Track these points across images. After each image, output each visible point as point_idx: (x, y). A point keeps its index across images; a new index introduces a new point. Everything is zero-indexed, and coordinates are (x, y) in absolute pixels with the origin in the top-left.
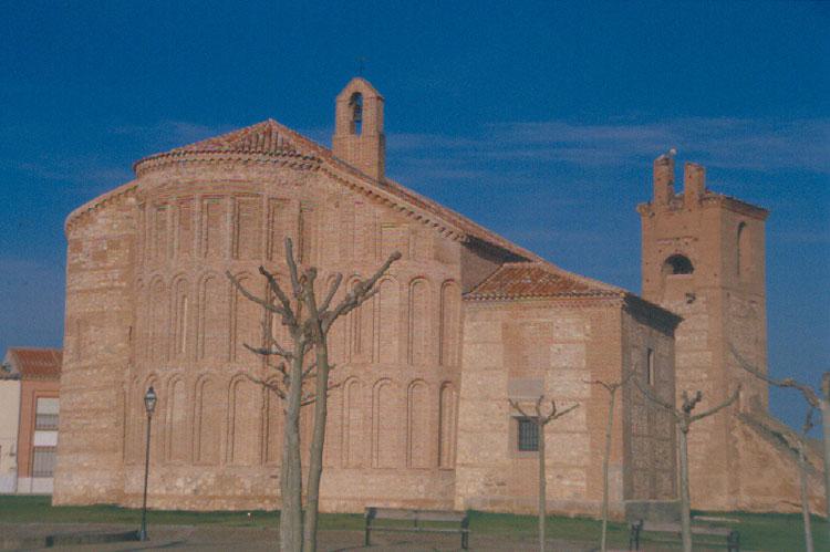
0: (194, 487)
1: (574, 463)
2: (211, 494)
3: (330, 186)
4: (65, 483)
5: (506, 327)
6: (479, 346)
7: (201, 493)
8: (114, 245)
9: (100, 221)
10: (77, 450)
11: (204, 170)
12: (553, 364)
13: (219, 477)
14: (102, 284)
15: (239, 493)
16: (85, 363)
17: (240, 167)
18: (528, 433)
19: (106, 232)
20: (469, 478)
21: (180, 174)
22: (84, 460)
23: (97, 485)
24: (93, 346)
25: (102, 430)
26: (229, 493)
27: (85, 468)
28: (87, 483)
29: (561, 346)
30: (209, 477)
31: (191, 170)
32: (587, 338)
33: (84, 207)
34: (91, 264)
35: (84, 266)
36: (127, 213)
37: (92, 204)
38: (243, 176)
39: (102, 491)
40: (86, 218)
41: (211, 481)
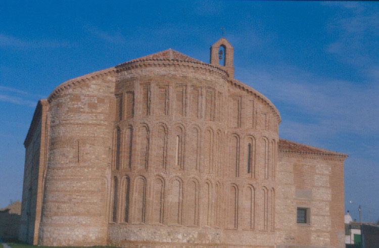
0: (188, 239)
1: (325, 230)
2: (196, 243)
3: (231, 90)
4: (68, 233)
5: (295, 165)
6: (283, 173)
7: (191, 242)
8: (101, 100)
9: (92, 86)
10: (78, 214)
11: (192, 72)
12: (315, 184)
13: (199, 234)
14: (94, 121)
15: (207, 242)
16: (82, 164)
17: (208, 74)
18: (303, 215)
19: (96, 93)
20: (278, 235)
21: (177, 71)
22: (83, 220)
23: (91, 235)
24: (88, 156)
25: (94, 203)
26: (204, 242)
27: (83, 225)
28: (85, 233)
29: (319, 176)
30: (194, 234)
31: (184, 70)
32: (330, 174)
33: (84, 77)
34: (87, 110)
35: (82, 110)
36: (108, 84)
37: (89, 76)
38: (209, 78)
39: (94, 238)
40: (83, 83)
41: (196, 236)
